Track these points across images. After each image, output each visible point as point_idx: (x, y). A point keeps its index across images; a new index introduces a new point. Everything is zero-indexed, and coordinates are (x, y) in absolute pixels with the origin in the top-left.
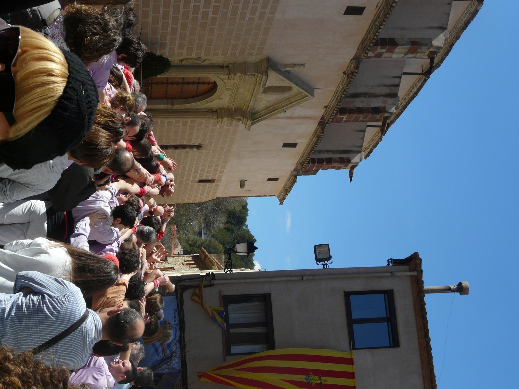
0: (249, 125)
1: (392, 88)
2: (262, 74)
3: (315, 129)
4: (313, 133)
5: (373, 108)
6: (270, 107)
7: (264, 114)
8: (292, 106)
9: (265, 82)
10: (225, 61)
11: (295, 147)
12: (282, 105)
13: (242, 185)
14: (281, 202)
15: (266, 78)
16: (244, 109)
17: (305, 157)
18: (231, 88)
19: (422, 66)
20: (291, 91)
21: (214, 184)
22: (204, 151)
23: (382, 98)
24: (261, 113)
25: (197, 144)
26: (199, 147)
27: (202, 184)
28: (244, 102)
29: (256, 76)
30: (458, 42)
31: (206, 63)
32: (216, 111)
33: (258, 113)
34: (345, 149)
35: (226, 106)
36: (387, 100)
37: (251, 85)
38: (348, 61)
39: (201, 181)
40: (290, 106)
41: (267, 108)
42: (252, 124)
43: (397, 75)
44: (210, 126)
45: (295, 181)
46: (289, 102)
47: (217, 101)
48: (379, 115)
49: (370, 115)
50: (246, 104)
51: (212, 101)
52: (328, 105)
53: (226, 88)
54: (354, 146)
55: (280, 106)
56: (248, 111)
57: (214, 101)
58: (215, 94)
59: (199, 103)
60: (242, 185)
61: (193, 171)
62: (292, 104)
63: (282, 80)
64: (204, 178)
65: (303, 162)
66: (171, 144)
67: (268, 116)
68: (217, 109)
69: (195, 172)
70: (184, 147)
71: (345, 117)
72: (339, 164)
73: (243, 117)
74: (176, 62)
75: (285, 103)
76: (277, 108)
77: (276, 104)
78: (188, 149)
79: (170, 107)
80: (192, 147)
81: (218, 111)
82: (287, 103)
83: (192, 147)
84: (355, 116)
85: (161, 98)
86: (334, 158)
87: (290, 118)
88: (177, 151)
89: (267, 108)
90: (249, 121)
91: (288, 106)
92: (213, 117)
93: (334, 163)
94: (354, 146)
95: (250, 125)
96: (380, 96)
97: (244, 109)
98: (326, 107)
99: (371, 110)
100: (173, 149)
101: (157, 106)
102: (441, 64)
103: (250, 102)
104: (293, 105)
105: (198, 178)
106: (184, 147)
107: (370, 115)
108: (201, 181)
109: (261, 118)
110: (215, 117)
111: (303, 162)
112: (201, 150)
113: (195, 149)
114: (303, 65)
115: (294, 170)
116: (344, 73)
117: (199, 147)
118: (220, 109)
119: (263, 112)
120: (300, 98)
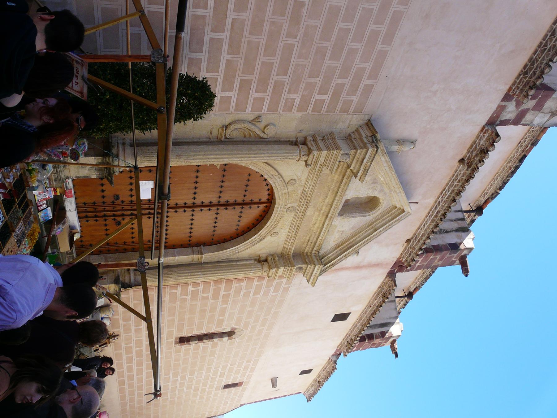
0: (315, 275)
1: (459, 222)
2: (365, 147)
3: (379, 285)
4: (375, 293)
5: (450, 244)
6: (343, 244)
7: (333, 256)
8: (377, 234)
9: (369, 164)
10: (301, 131)
11: (345, 319)
12: (361, 237)
13: (274, 384)
14: (309, 398)
15: (374, 153)
16: (305, 252)
17: (356, 331)
18: (295, 205)
19: (469, 204)
20: (377, 210)
21: (241, 388)
22: (236, 339)
23: (454, 233)
24: (329, 257)
25: (228, 330)
26: (230, 334)
27: (227, 390)
28: (308, 238)
29: (351, 157)
30: (535, 148)
31: (270, 133)
32: (266, 260)
33: (325, 256)
34: (383, 322)
35: (279, 250)
36: (460, 235)
37: (327, 197)
38: (479, 128)
39: (226, 387)
40: (375, 235)
41: (338, 247)
42: (322, 272)
43: (457, 210)
44: (251, 294)
45: (334, 369)
46: (372, 230)
47: (269, 238)
48: (456, 254)
49: (448, 255)
50: (311, 240)
51: (261, 240)
52: (412, 238)
53: (289, 206)
54: (390, 318)
55: (358, 239)
56: (313, 252)
57: (264, 241)
58: (268, 224)
59: (242, 246)
60: (274, 384)
61: (219, 374)
62: (378, 231)
63: (362, 195)
64: (230, 382)
65: (351, 339)
66: (195, 332)
67: (340, 259)
68: (267, 257)
69: (222, 375)
70: (210, 336)
71: (420, 260)
72: (380, 340)
73: (306, 263)
74: (215, 133)
75: (366, 232)
76: (354, 242)
77: (353, 237)
78: (216, 340)
79: (196, 257)
80: (221, 335)
81: (269, 259)
82: (369, 232)
83: (221, 335)
84: (431, 257)
85: (182, 246)
86: (375, 333)
87: (358, 267)
88: (201, 345)
89: (337, 247)
90: (317, 267)
91: (372, 235)
92: (263, 268)
93: (376, 338)
94: (390, 318)
95: (318, 275)
96: (451, 231)
97: (305, 252)
98: (408, 241)
99: (449, 248)
100: (197, 342)
101: (177, 258)
102: (500, 192)
103: (320, 233)
104: (379, 232)
105: (223, 384)
106: (210, 336)
107: (448, 255)
108: (226, 387)
109: (330, 264)
110: (266, 268)
111: (351, 339)
112: (233, 338)
113: (225, 339)
114: (413, 142)
115: (333, 355)
116: (462, 161)
117: (230, 334)
118: (271, 255)
119: (331, 254)
120: (390, 218)
